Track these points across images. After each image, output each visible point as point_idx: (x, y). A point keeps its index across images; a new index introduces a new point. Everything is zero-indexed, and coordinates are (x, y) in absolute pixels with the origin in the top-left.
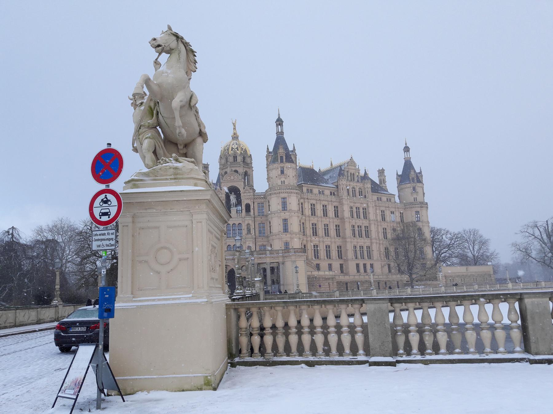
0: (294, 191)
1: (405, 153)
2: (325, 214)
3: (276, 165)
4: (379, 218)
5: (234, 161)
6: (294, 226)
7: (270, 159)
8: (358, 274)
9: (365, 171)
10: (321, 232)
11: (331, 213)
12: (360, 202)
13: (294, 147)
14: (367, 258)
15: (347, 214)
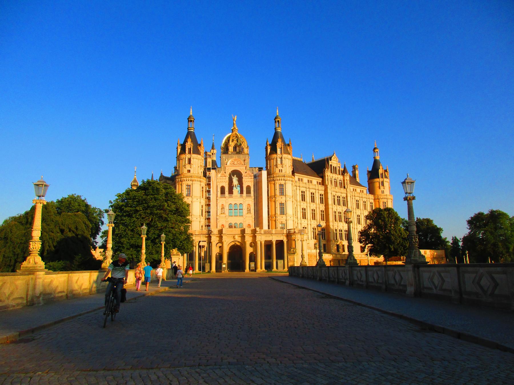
0: (290, 178)
1: (374, 153)
2: (313, 200)
3: (274, 156)
4: (355, 206)
5: (234, 151)
6: (290, 210)
7: (269, 151)
8: (338, 253)
9: (345, 166)
10: (309, 215)
11: (317, 200)
12: (341, 192)
13: (290, 141)
14: (345, 240)
15: (330, 201)
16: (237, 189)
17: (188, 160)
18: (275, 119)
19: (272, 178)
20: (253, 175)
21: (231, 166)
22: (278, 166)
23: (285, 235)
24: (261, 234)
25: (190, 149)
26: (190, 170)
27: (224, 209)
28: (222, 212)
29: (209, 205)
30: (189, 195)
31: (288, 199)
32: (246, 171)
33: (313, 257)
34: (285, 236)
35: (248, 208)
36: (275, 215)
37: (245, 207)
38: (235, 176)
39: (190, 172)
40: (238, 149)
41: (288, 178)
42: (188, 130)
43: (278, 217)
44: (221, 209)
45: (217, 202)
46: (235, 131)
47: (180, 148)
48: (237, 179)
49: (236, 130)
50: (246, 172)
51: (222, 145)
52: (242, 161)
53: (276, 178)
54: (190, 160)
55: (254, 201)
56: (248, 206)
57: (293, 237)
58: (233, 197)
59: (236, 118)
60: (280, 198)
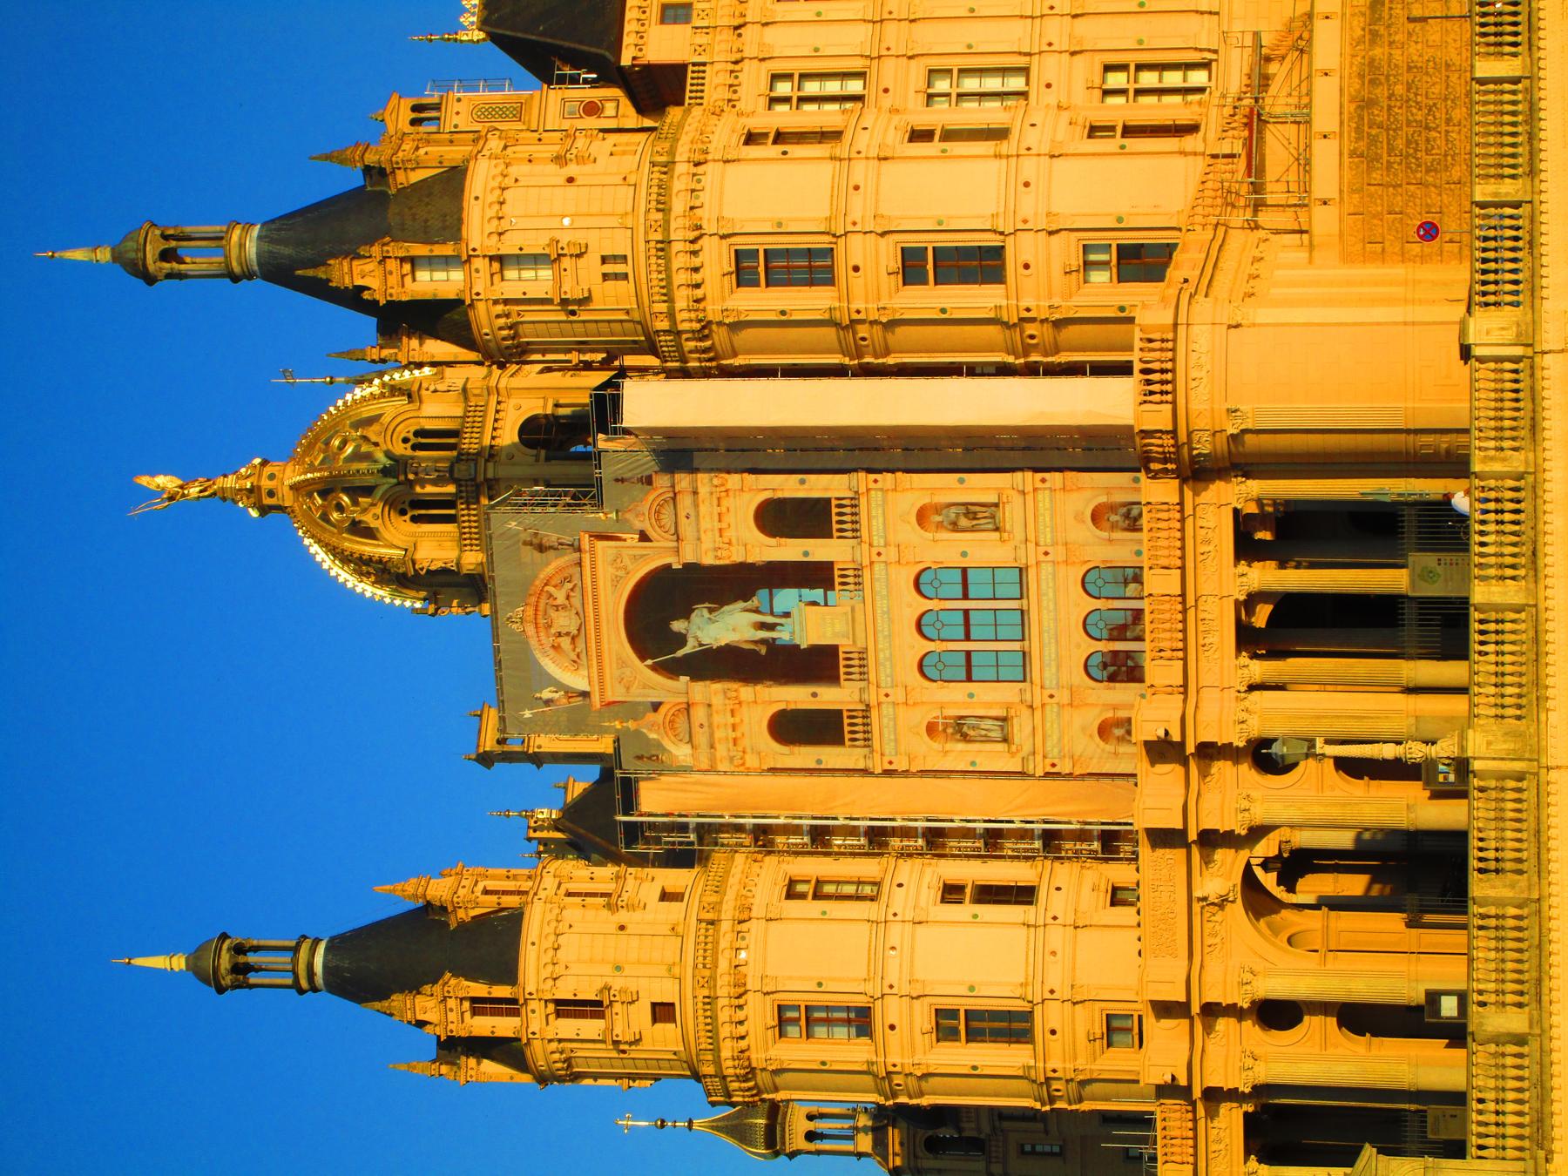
3: (485, 320)
16: (787, 615)
17: (568, 1015)
18: (150, 280)
19: (679, 347)
20: (662, 481)
21: (599, 657)
22: (572, 291)
23: (1188, 494)
24: (1185, 686)
25: (474, 1000)
26: (654, 1005)
27: (972, 722)
28: (996, 734)
29: (936, 840)
30: (861, 1020)
31: (859, 209)
32: (632, 539)
33: (1378, 52)
34: (1196, 494)
35: (955, 527)
36: (1006, 325)
37: (949, 549)
38: (678, 626)
39: (672, 1005)
40: (430, 489)
41: (678, 205)
42: (314, 989)
43: (1024, 304)
44: (961, 746)
45: (906, 774)
46: (271, 494)
47: (472, 1062)
48: (700, 614)
49: (266, 484)
50: (644, 537)
51: (408, 604)
52: (550, 570)
53: (685, 315)
54: (567, 1008)
55: (893, 471)
56: (940, 525)
57: (1203, 446)
58: (860, 644)
59: (161, 480)
60: (857, 281)
